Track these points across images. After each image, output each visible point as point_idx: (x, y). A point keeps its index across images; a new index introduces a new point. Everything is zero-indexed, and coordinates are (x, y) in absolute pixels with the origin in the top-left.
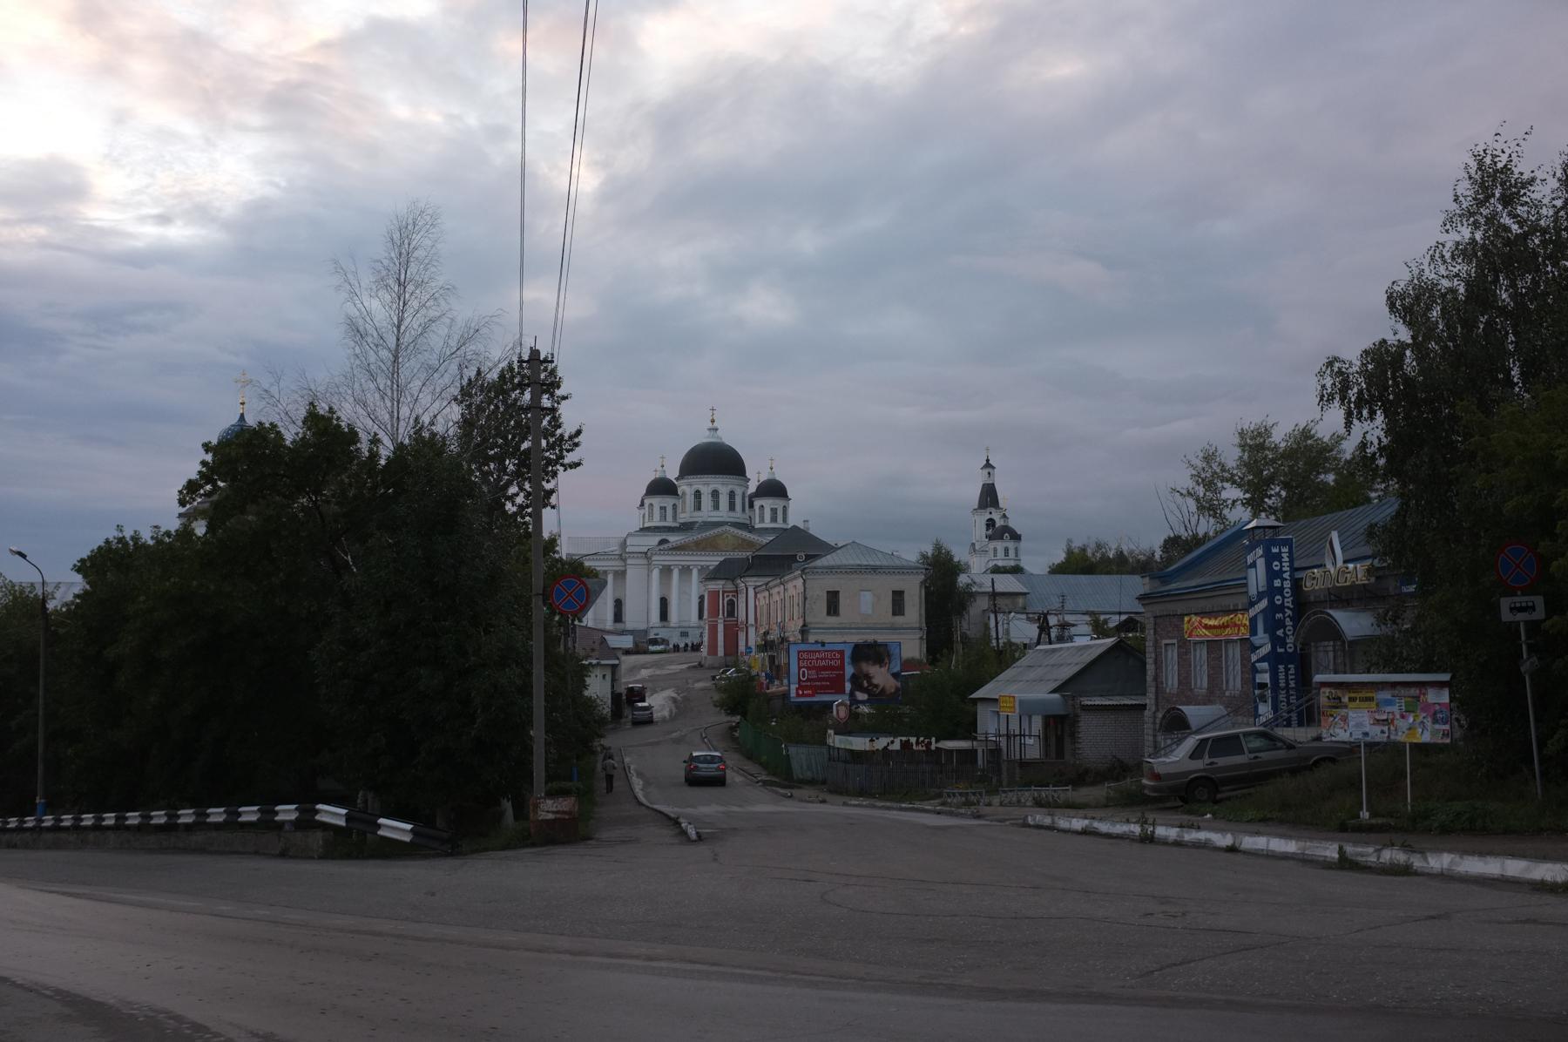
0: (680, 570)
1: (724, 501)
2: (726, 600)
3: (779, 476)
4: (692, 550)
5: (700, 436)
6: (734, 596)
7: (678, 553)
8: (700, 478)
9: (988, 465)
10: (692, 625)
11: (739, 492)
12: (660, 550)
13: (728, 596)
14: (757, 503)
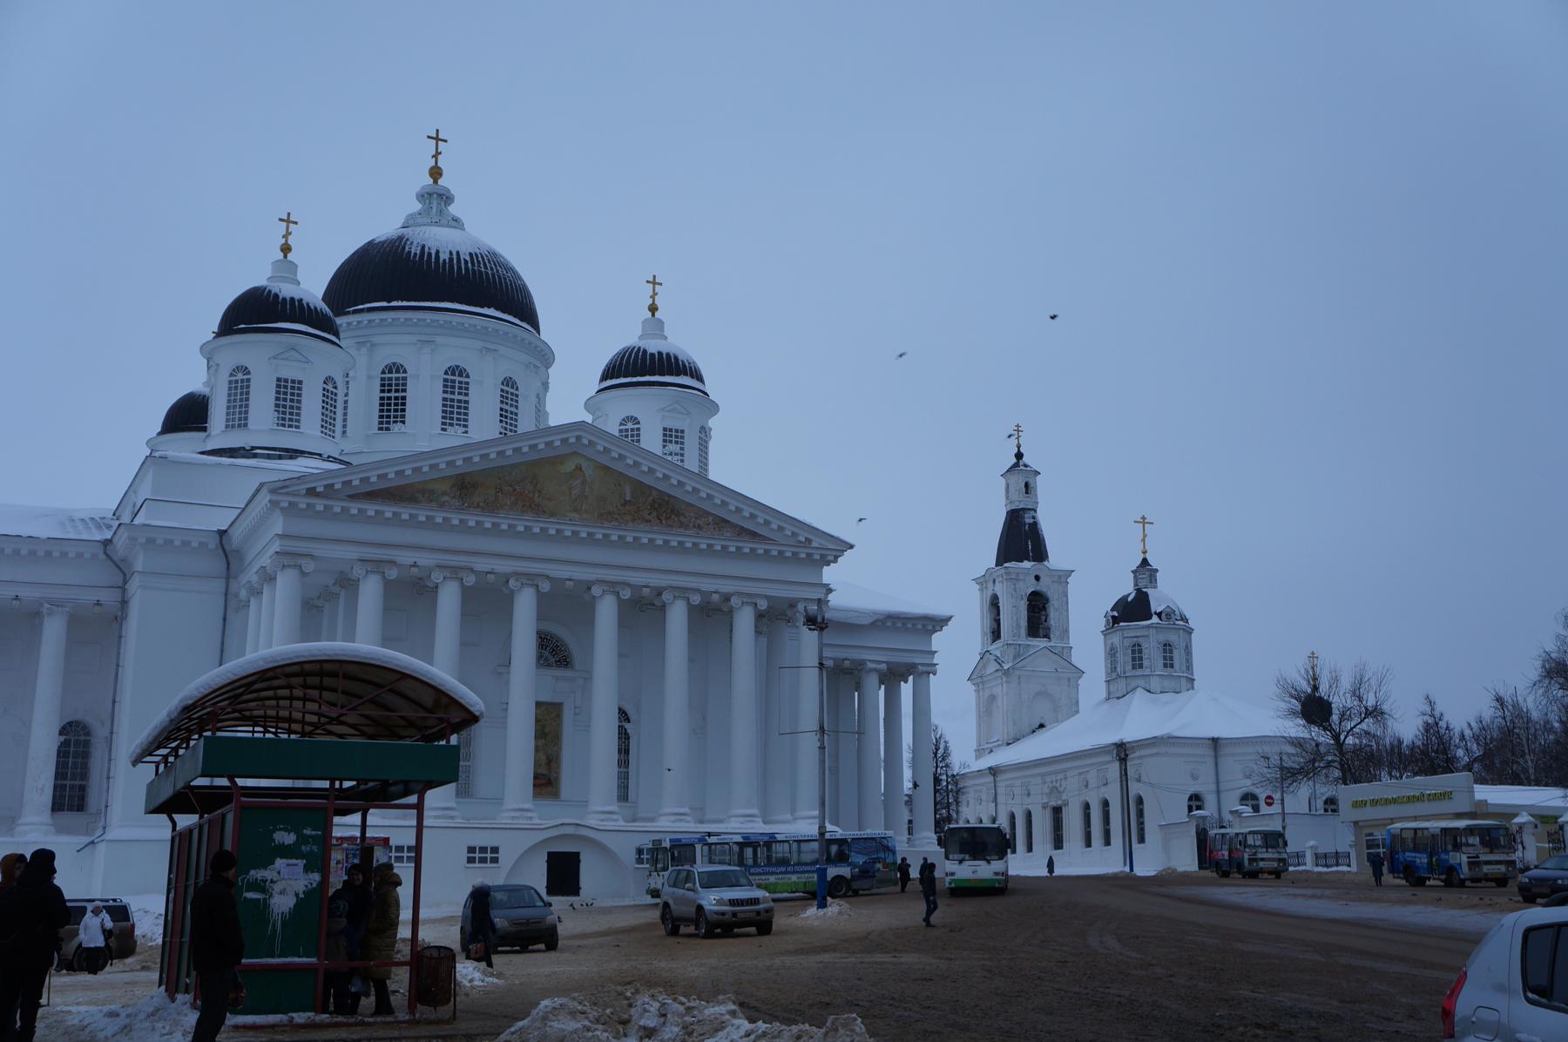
3: (679, 341)
4: (442, 505)
7: (389, 511)
11: (526, 388)
12: (311, 492)
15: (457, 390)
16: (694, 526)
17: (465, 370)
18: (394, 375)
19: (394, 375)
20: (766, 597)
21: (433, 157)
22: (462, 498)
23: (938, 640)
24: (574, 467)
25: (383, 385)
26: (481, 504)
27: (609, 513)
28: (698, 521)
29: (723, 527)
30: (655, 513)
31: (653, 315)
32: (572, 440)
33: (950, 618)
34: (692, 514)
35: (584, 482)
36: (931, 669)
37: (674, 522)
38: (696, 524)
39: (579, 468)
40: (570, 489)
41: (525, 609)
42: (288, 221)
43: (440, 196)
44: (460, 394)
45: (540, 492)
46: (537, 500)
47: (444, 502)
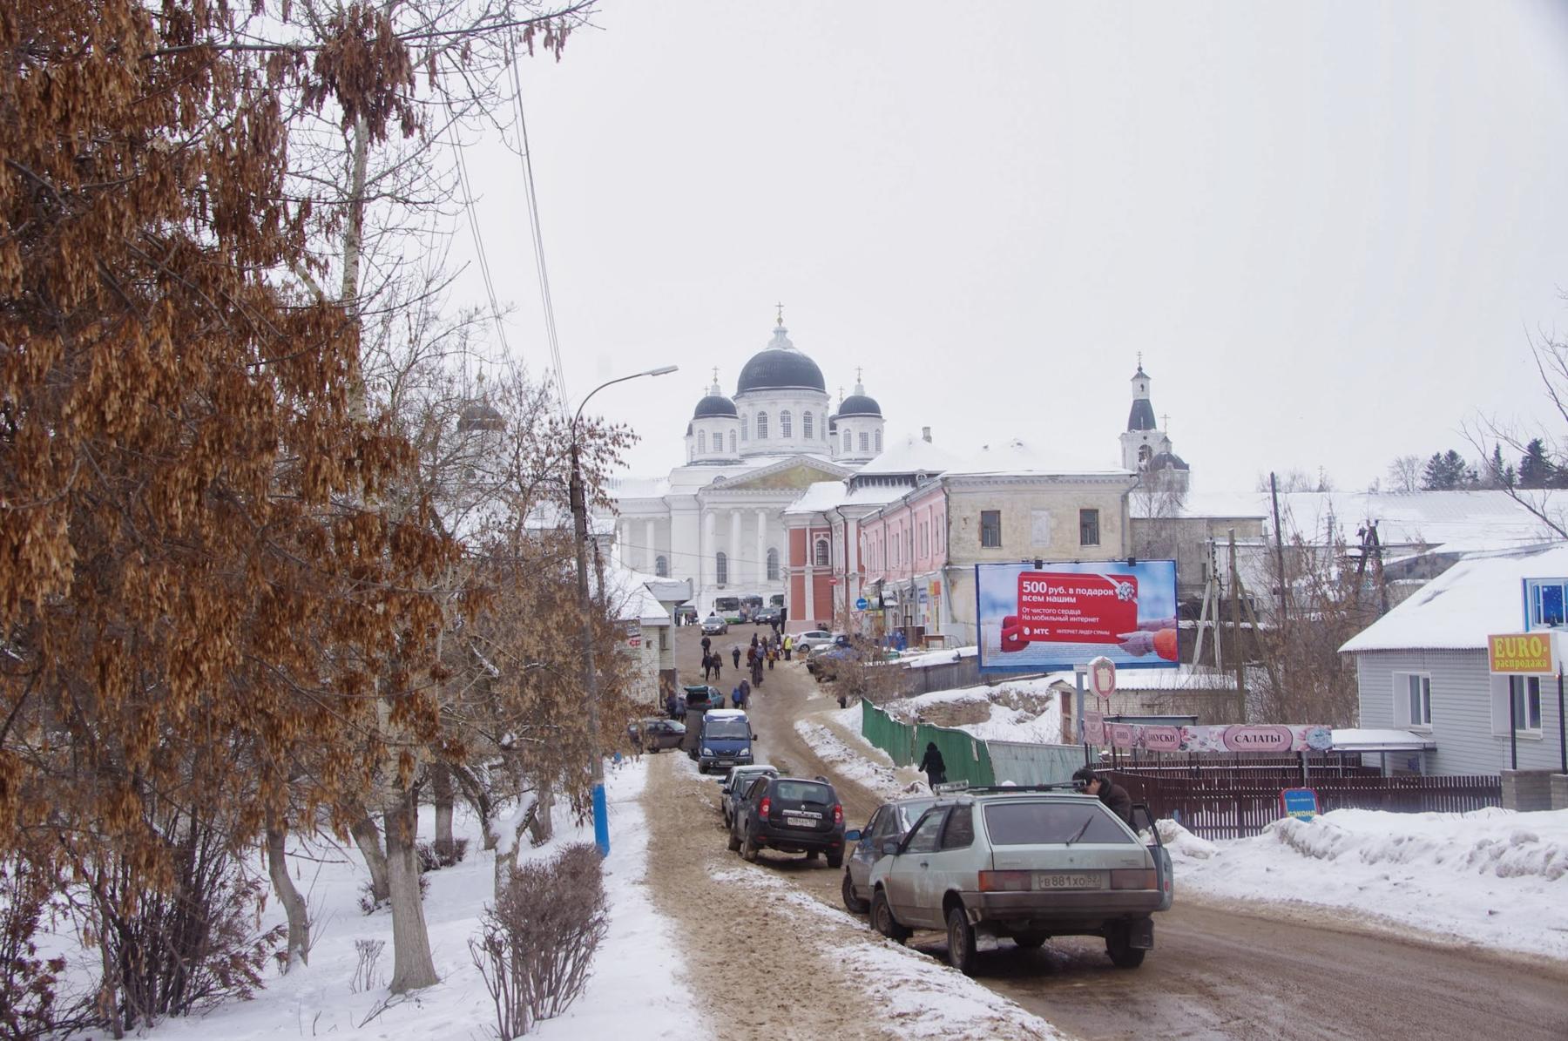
1: (797, 426)
2: (816, 541)
3: (869, 393)
5: (759, 343)
6: (825, 536)
9: (1140, 375)
13: (818, 536)
14: (842, 425)
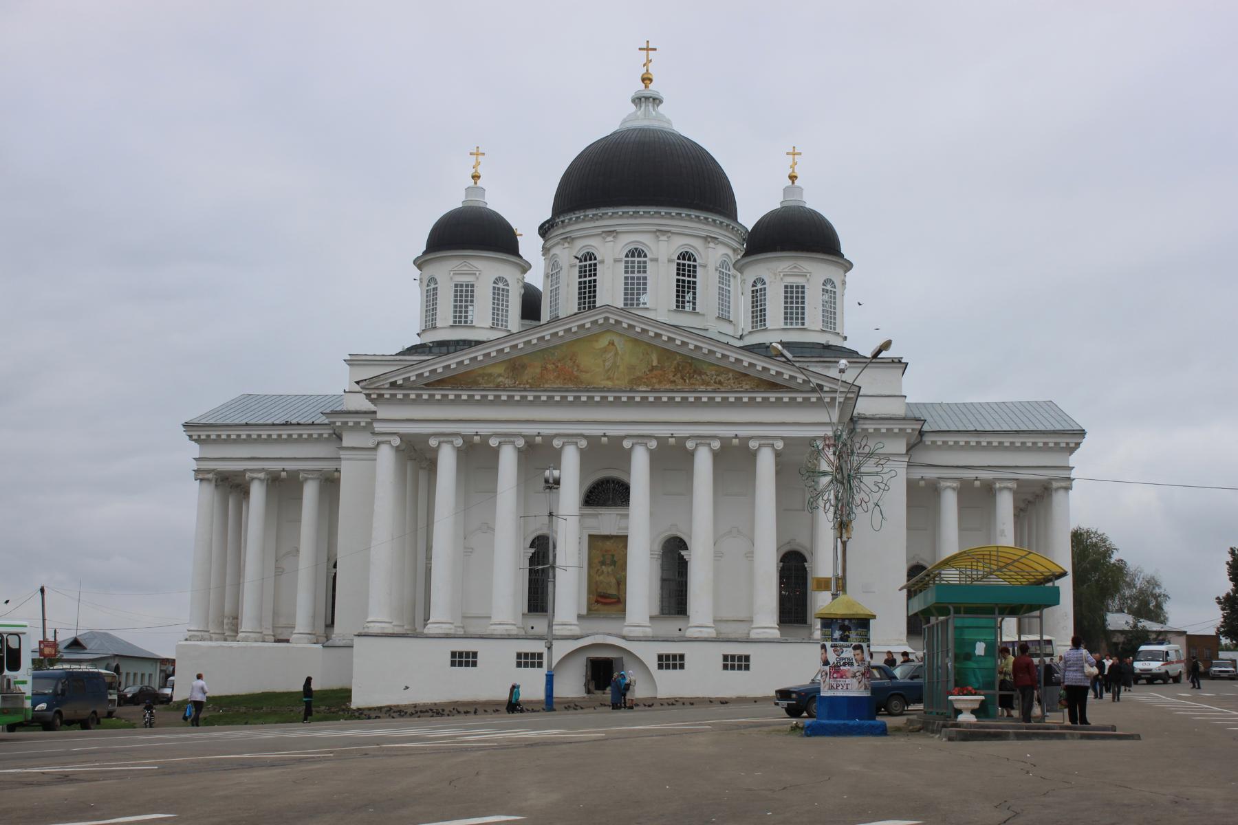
0: (458, 450)
4: (498, 387)
8: (595, 218)
10: (492, 629)
12: (393, 385)
15: (636, 270)
16: (715, 383)
17: (643, 251)
18: (588, 263)
19: (588, 263)
20: (782, 438)
21: (644, 65)
22: (514, 378)
23: (1073, 460)
24: (607, 343)
25: (580, 272)
26: (530, 381)
27: (639, 378)
28: (719, 378)
29: (742, 380)
30: (679, 375)
31: (793, 183)
32: (601, 321)
33: (1082, 433)
34: (713, 372)
35: (616, 354)
36: (1067, 486)
37: (697, 380)
38: (717, 380)
39: (612, 343)
40: (604, 361)
41: (570, 463)
42: (477, 154)
43: (647, 98)
44: (639, 272)
45: (578, 366)
46: (575, 373)
47: (499, 383)
